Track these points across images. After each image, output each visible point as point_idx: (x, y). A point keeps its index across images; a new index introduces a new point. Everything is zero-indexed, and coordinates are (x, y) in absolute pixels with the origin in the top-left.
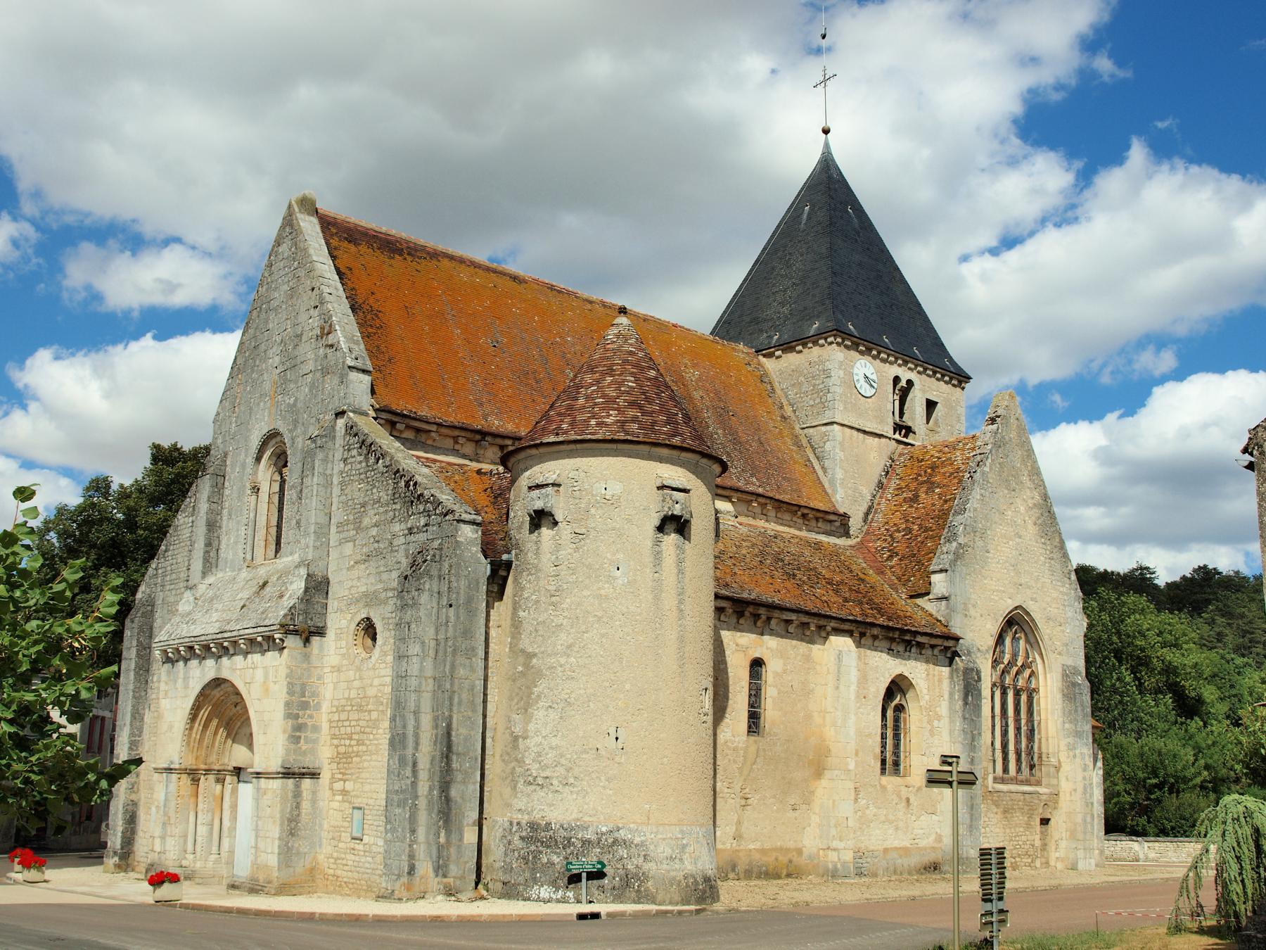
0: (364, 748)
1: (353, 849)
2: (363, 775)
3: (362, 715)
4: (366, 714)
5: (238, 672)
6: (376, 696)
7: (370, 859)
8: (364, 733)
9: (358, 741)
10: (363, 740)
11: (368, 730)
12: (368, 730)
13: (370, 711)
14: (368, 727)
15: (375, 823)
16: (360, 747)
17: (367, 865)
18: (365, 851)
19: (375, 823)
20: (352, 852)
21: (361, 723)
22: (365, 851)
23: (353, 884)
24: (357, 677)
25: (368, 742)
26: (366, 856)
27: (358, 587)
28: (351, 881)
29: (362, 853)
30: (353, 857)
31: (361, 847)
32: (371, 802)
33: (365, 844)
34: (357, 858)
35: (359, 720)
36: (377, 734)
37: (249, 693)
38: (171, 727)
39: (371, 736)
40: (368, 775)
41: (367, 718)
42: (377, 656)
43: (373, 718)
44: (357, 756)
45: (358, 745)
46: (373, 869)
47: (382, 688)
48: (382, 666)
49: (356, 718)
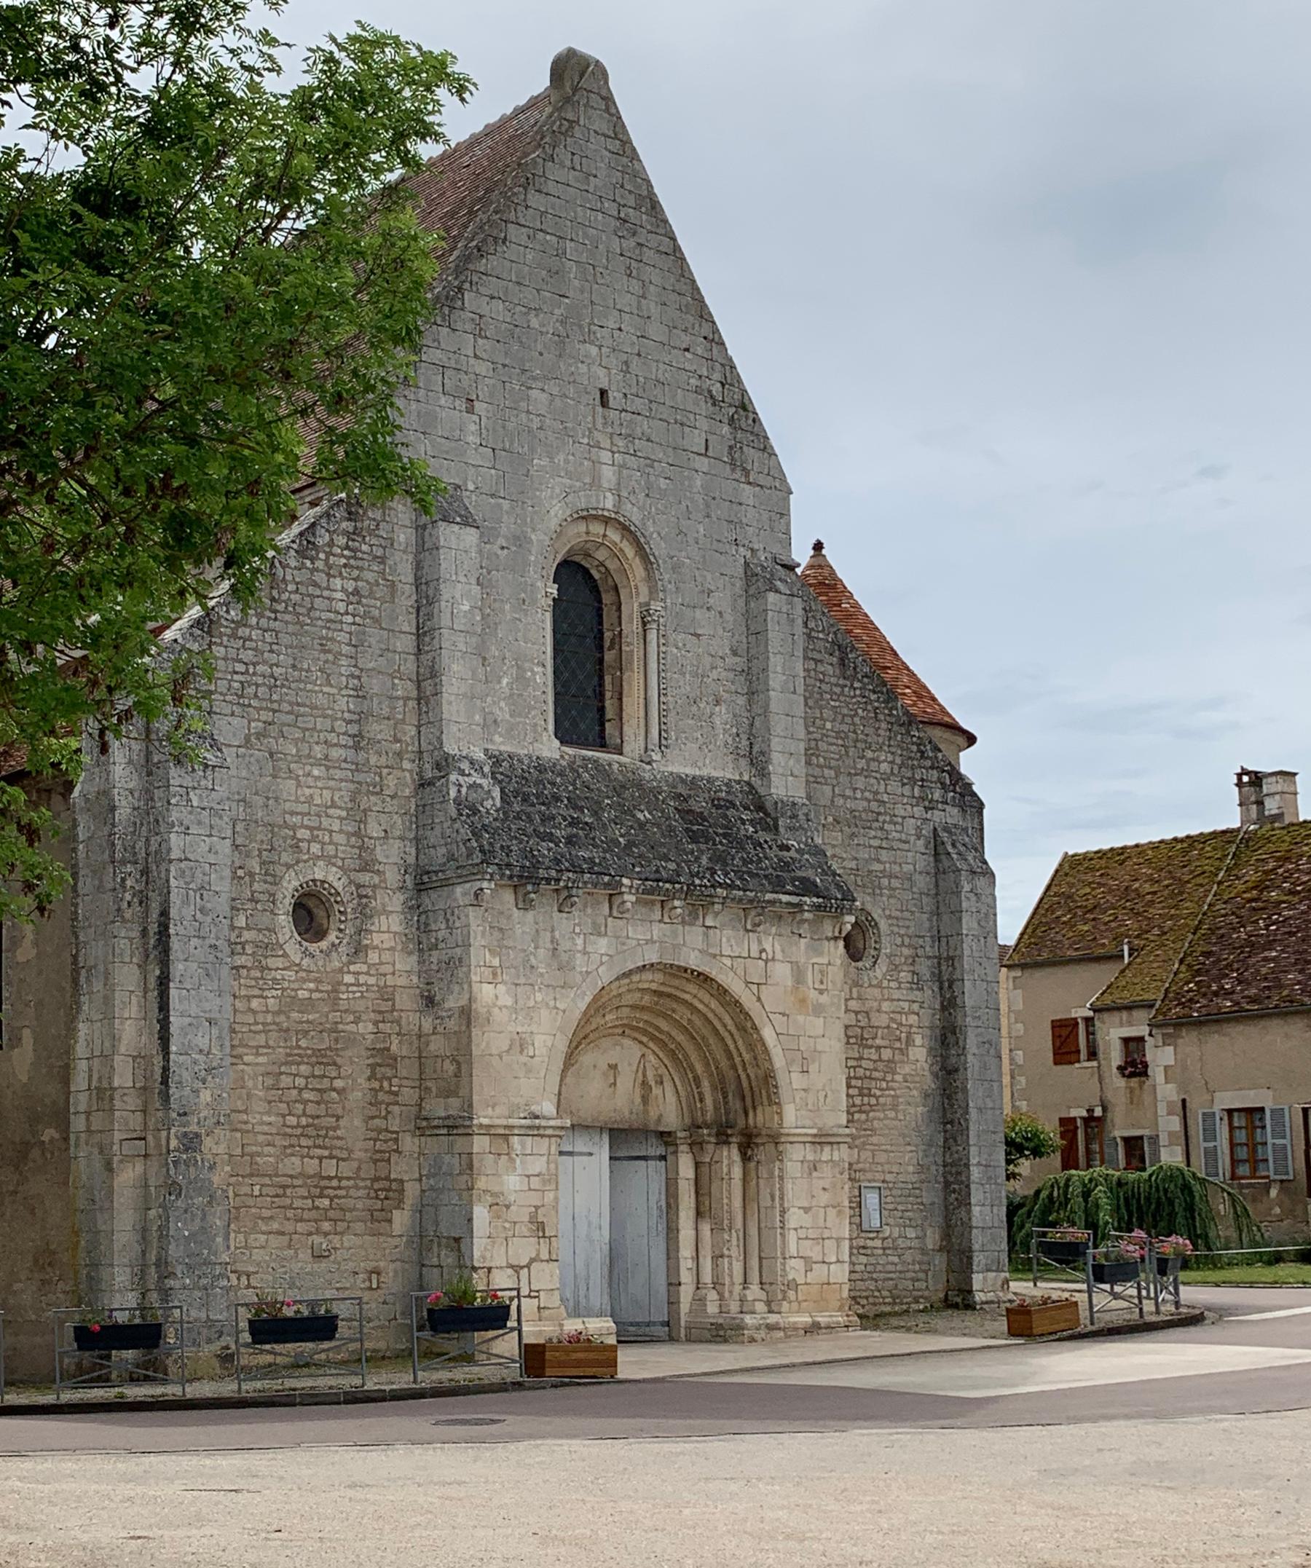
0: (873, 1101)
1: (864, 1247)
2: (875, 1140)
3: (866, 1053)
4: (873, 1050)
5: (728, 962)
6: (888, 1027)
7: (896, 1259)
8: (870, 1078)
9: (860, 1089)
10: (870, 1089)
11: (876, 1074)
12: (876, 1074)
13: (879, 1048)
14: (876, 1070)
15: (900, 1207)
16: (866, 1099)
17: (890, 1268)
18: (884, 1249)
19: (900, 1207)
20: (862, 1251)
21: (864, 1063)
22: (884, 1249)
23: (867, 1298)
24: (855, 995)
25: (878, 1093)
26: (887, 1255)
27: (844, 860)
28: (864, 1294)
29: (880, 1252)
30: (864, 1259)
31: (878, 1243)
32: (889, 1177)
33: (884, 1239)
34: (872, 1260)
35: (861, 1058)
36: (893, 1081)
37: (759, 999)
38: (521, 1044)
39: (884, 1085)
40: (883, 1140)
41: (875, 1057)
42: (884, 969)
43: (885, 1057)
44: (860, 1112)
45: (861, 1095)
46: (900, 1272)
47: (897, 1017)
48: (893, 984)
49: (857, 1055)
